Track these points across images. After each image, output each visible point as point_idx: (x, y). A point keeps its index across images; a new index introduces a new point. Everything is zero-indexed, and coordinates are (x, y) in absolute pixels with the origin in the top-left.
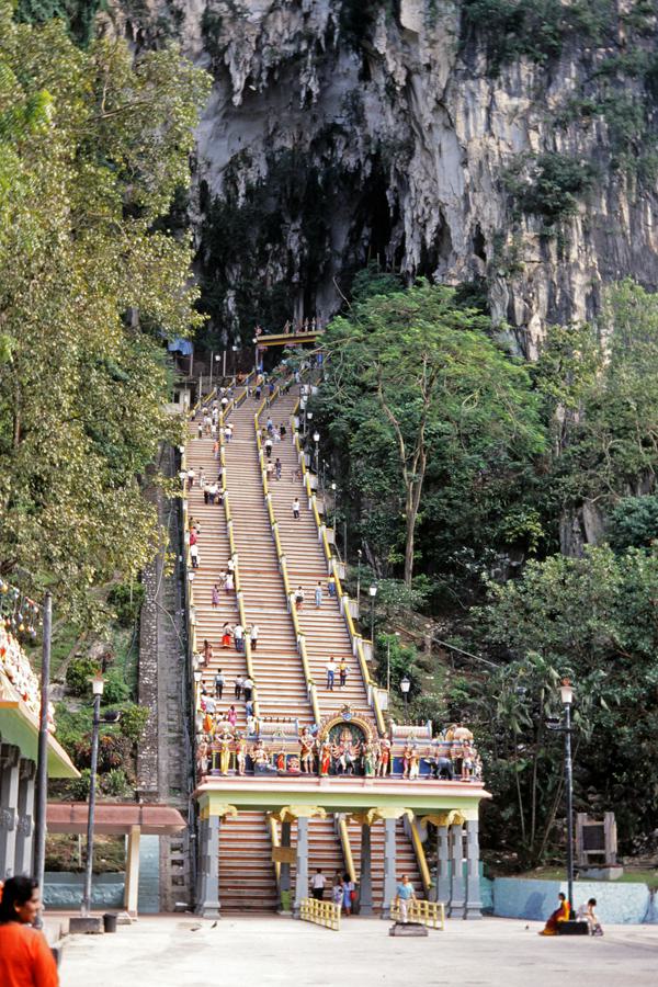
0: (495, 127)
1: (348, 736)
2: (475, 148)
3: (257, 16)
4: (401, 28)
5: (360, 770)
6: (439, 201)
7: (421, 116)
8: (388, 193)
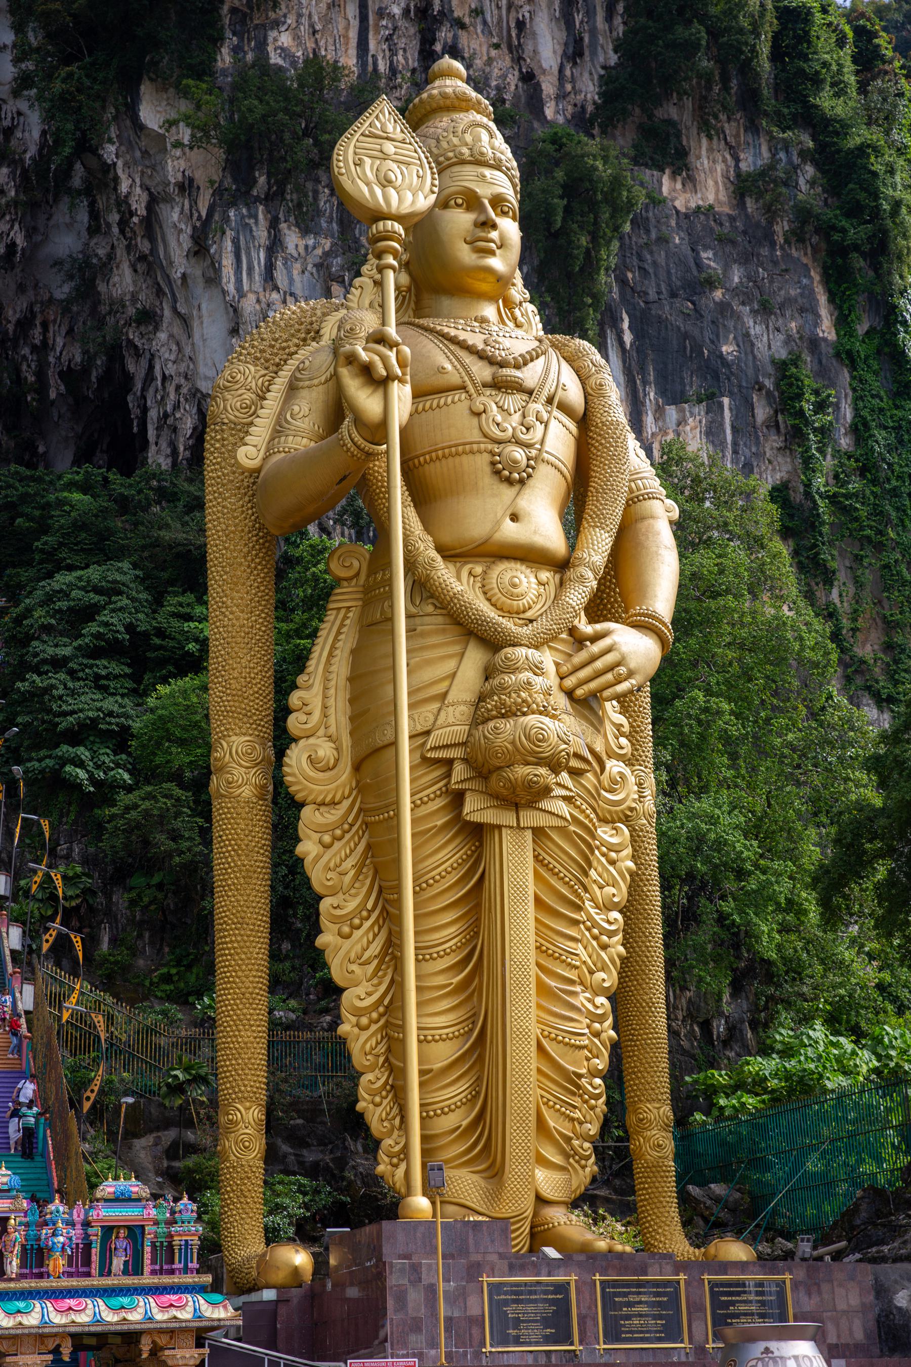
0: (280, 276)
2: (249, 305)
4: (139, 127)
6: (198, 390)
7: (171, 263)
8: (130, 398)
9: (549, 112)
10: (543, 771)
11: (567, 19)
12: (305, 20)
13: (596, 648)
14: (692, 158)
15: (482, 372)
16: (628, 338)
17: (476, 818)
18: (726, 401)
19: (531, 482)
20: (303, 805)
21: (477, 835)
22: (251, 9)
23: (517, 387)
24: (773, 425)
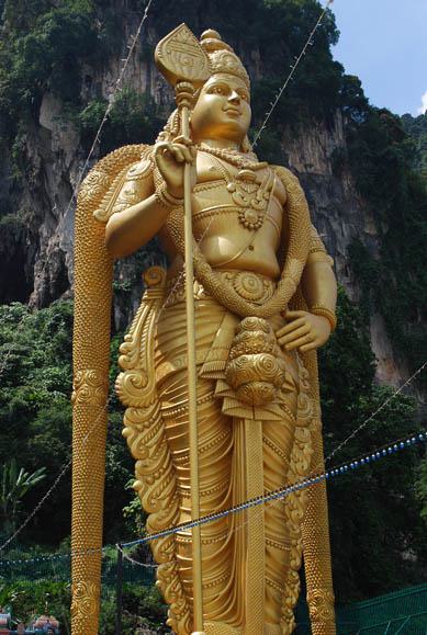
4: (40, 126)
7: (50, 191)
10: (270, 386)
20: (127, 407)
21: (229, 424)
22: (94, 74)
23: (253, 181)
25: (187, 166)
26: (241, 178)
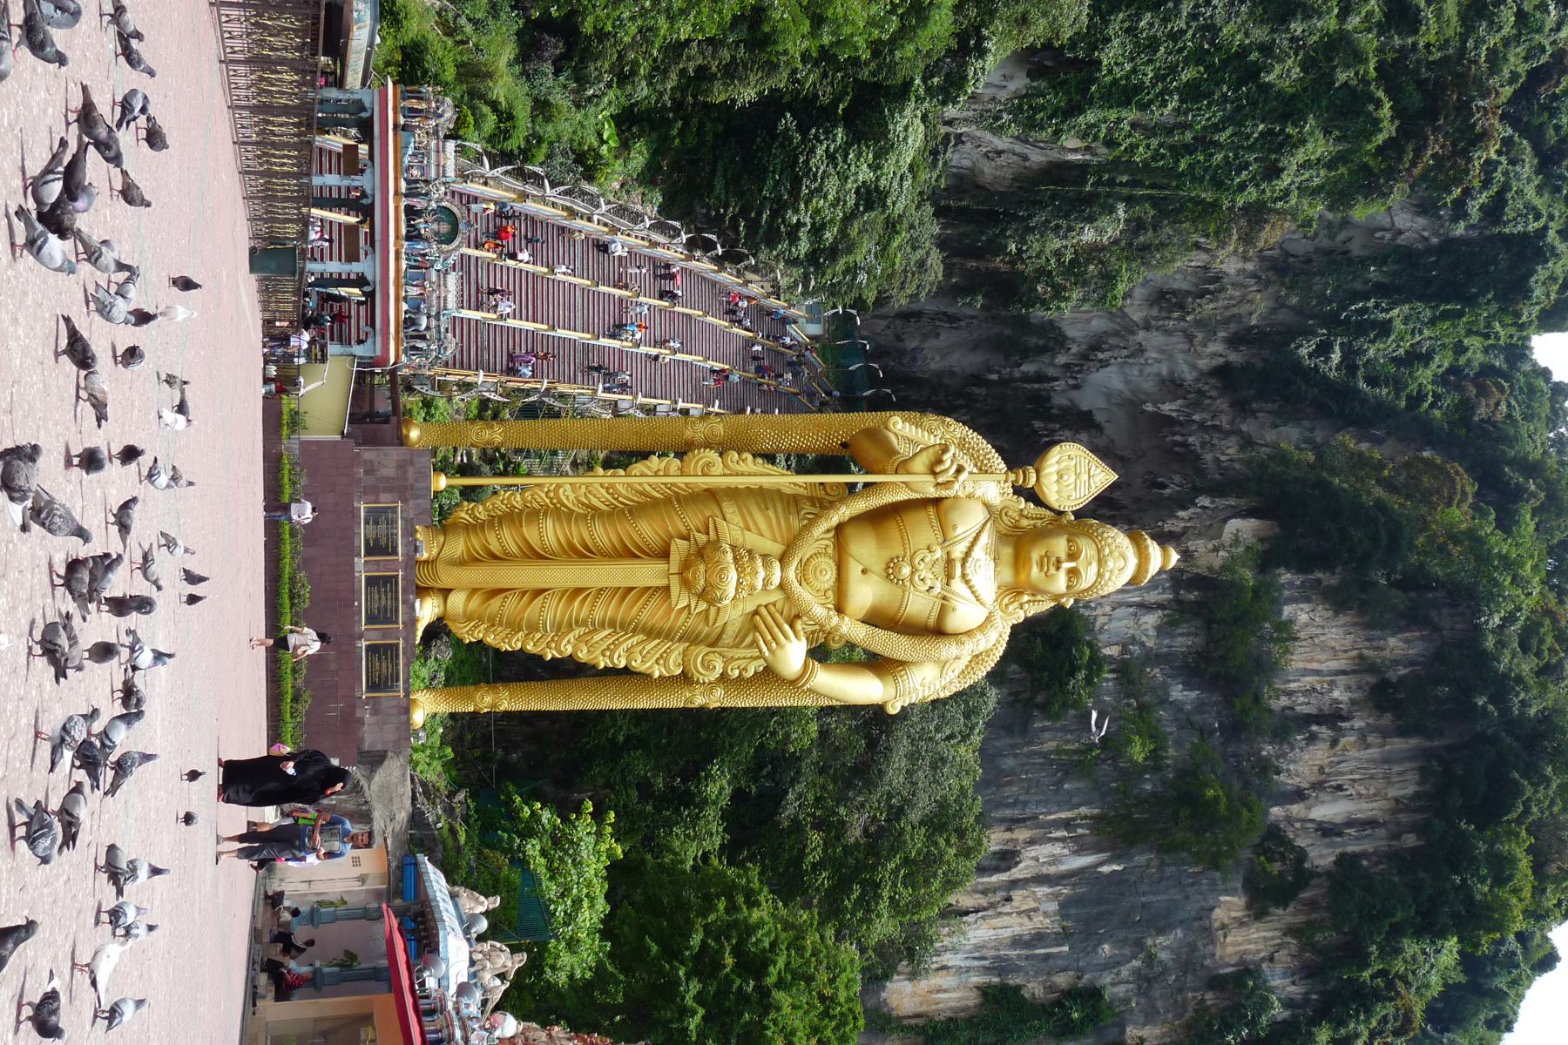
1: (445, 228)
3: (1244, 428)
4: (1225, 521)
5: (413, 236)
9: (1276, 811)
10: (702, 582)
11: (1350, 823)
12: (1320, 631)
13: (786, 627)
14: (1257, 925)
15: (958, 552)
16: (1105, 869)
17: (673, 548)
18: (1066, 948)
19: (889, 585)
23: (949, 577)
24: (1051, 988)
25: (930, 478)
26: (949, 562)
